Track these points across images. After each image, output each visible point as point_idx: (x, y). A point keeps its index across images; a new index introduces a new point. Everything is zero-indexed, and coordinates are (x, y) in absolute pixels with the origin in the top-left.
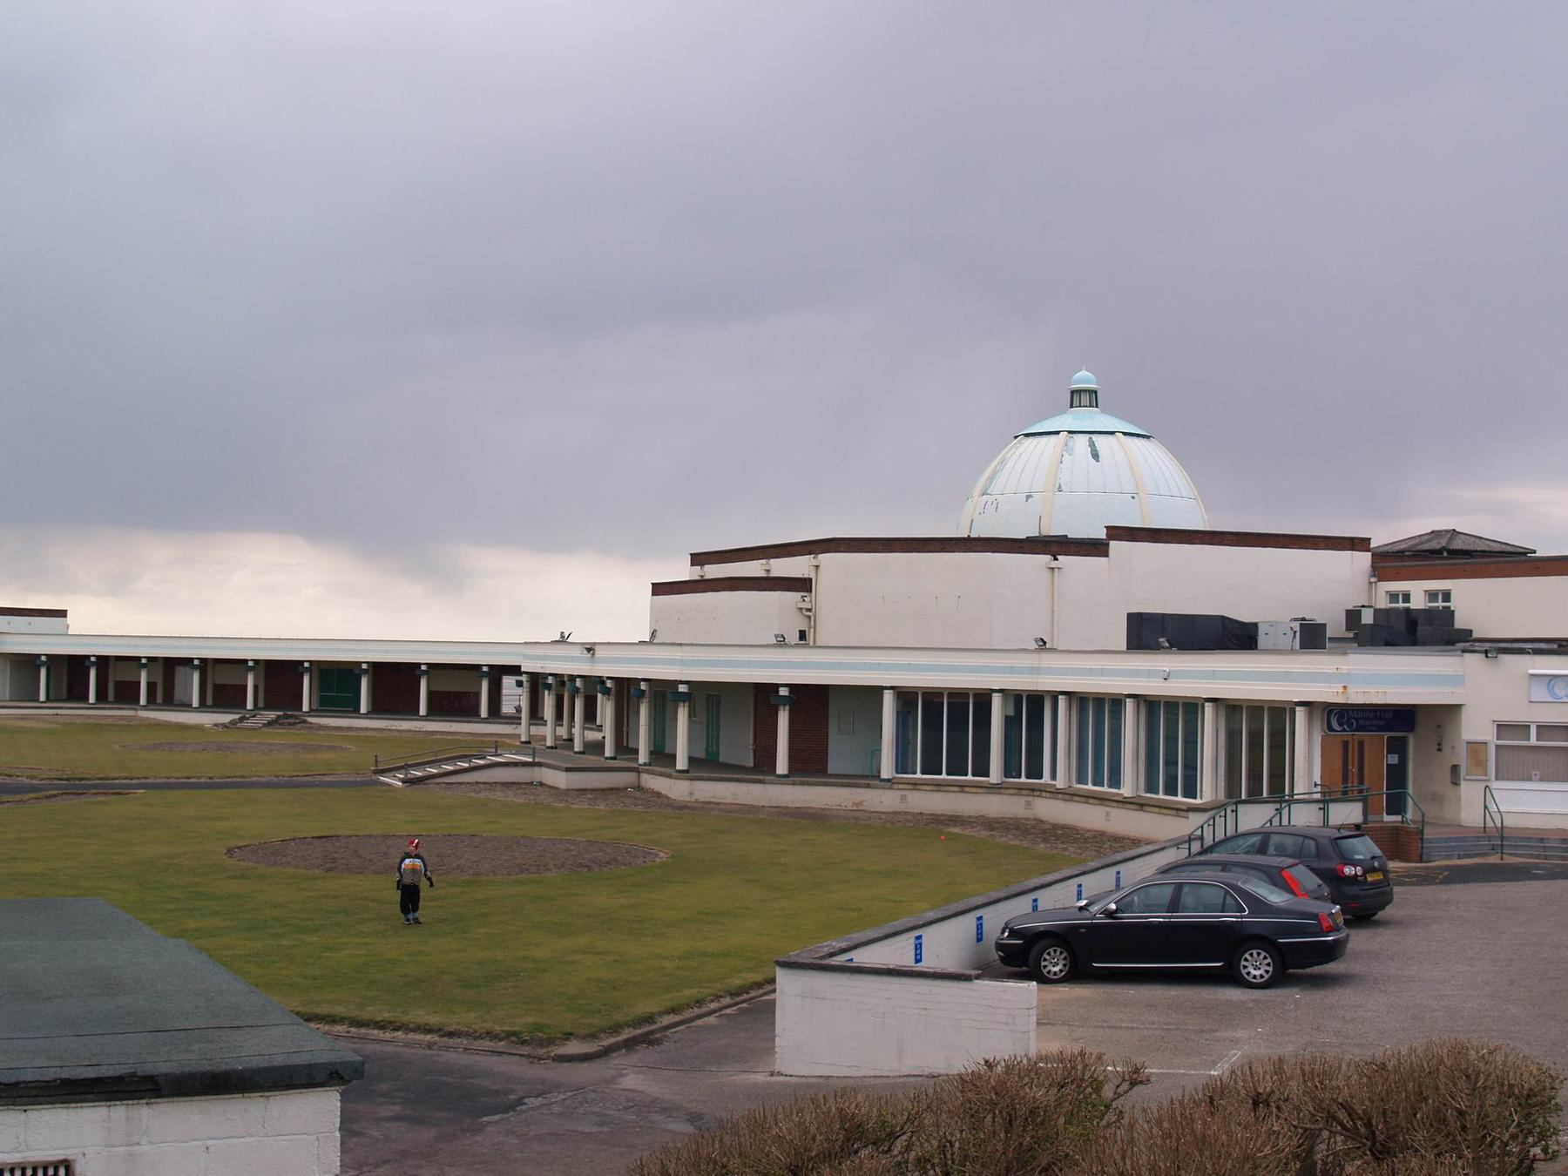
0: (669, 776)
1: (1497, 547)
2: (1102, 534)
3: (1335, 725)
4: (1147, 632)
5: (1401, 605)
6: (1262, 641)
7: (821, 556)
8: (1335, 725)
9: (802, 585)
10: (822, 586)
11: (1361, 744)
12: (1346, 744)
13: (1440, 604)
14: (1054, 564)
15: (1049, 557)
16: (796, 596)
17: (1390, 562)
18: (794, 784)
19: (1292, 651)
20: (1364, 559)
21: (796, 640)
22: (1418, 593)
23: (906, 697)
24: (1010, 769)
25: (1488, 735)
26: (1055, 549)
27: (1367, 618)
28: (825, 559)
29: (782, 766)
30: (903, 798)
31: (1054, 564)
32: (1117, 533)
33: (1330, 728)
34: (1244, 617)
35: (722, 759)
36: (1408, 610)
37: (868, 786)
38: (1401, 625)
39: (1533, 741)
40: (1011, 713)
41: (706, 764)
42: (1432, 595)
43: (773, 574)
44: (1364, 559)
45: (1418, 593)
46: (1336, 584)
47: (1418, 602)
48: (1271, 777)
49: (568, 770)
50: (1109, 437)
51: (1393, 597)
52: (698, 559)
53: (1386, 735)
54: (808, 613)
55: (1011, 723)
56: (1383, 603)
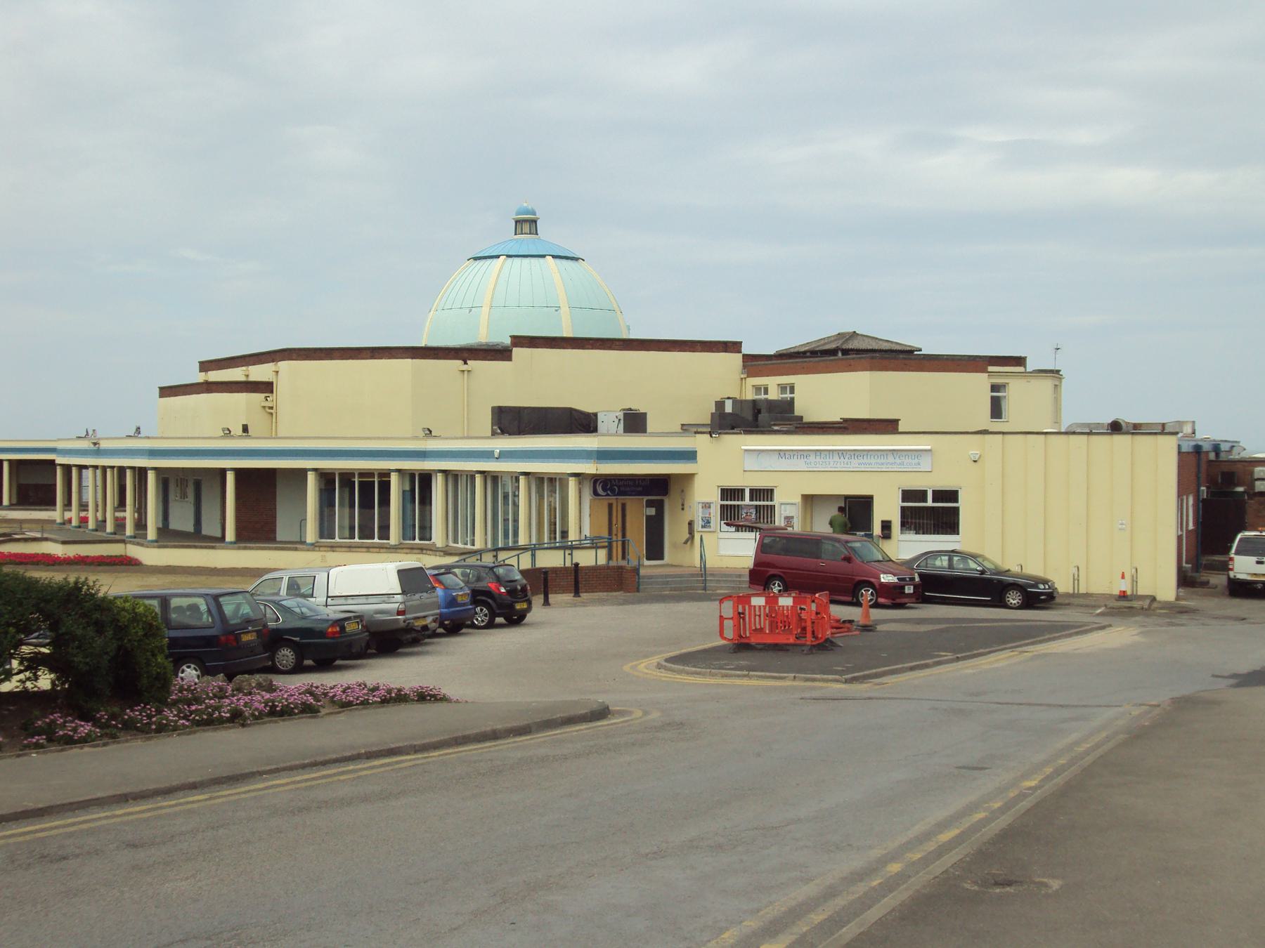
0: (142, 545)
1: (875, 346)
2: (508, 341)
3: (600, 490)
4: (512, 420)
5: (763, 396)
6: (651, 426)
7: (281, 364)
8: (600, 490)
9: (266, 387)
10: (281, 388)
11: (624, 506)
12: (610, 506)
13: (788, 396)
14: (465, 367)
15: (460, 362)
16: (259, 397)
17: (755, 365)
18: (239, 548)
19: (616, 434)
20: (736, 359)
21: (240, 432)
22: (773, 387)
23: (326, 478)
24: (407, 532)
25: (715, 498)
26: (466, 355)
27: (729, 408)
28: (284, 365)
29: (230, 535)
30: (323, 558)
31: (465, 367)
32: (520, 341)
33: (595, 493)
34: (588, 409)
35: (204, 532)
36: (766, 400)
37: (296, 549)
38: (748, 415)
39: (930, 503)
40: (407, 488)
41: (168, 535)
42: (783, 388)
43: (252, 379)
44: (736, 359)
45: (773, 387)
46: (723, 380)
47: (774, 395)
48: (380, 528)
49: (64, 543)
50: (541, 260)
51: (757, 389)
52: (206, 366)
53: (646, 498)
54: (270, 411)
55: (408, 497)
56: (750, 395)
